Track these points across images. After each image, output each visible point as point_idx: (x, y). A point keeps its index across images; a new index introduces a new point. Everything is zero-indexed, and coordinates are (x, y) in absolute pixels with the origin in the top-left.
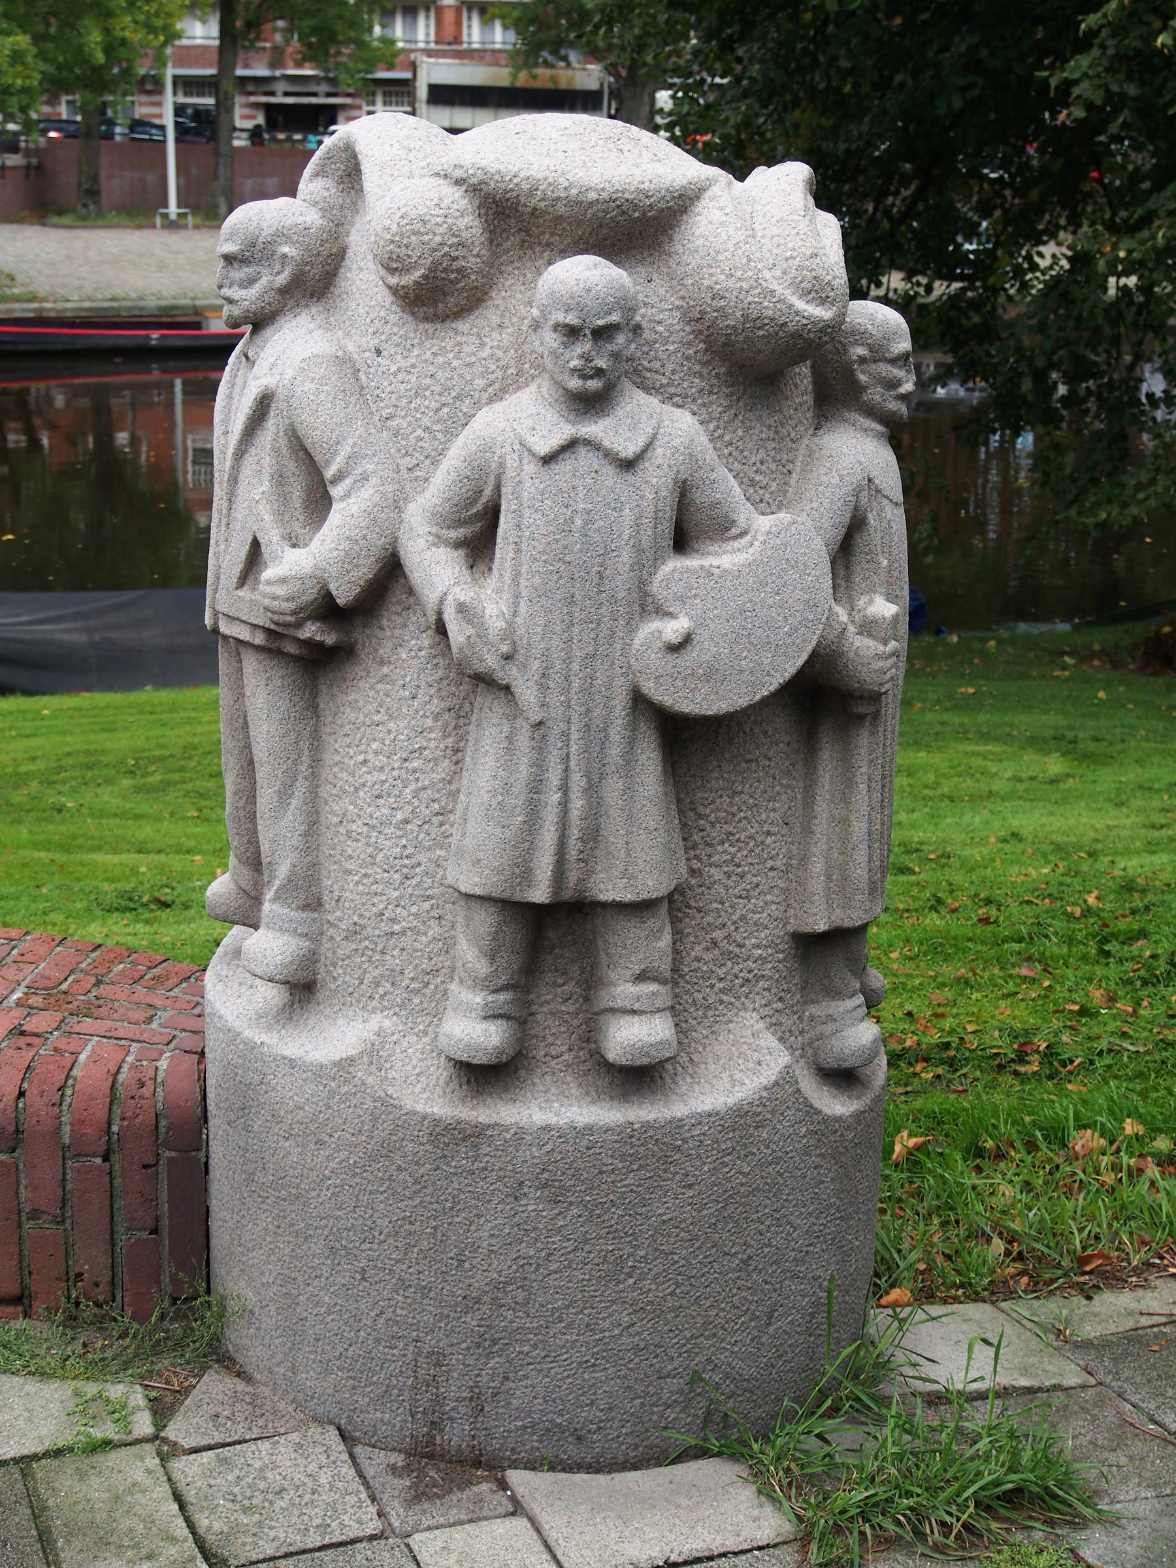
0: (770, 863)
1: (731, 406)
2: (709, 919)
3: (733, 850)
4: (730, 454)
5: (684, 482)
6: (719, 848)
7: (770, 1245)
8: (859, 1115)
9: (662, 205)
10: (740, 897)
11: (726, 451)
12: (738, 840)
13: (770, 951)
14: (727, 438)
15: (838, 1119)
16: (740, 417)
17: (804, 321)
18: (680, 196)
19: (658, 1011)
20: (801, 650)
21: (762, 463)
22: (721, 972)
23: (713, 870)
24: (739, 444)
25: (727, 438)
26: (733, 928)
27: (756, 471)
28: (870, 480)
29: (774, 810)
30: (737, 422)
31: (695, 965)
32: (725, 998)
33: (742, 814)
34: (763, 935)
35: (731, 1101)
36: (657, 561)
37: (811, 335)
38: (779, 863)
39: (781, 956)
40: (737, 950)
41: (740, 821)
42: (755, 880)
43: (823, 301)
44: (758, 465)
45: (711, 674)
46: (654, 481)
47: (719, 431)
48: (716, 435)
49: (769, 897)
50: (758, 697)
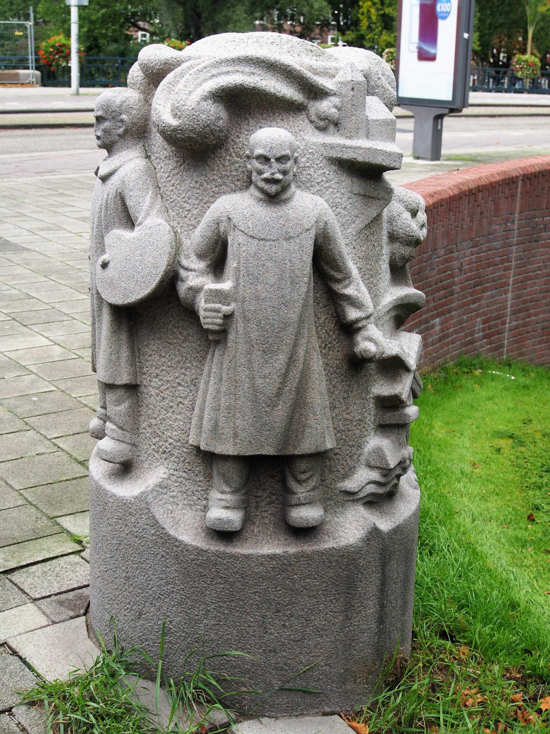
0: (179, 400)
1: (176, 167)
2: (150, 412)
3: (160, 383)
4: (172, 190)
5: (120, 193)
6: (154, 379)
7: (138, 578)
8: (200, 551)
9: (157, 67)
10: (162, 408)
11: (171, 188)
12: (162, 379)
13: (178, 444)
14: (172, 182)
15: (180, 542)
16: (181, 173)
17: (164, 125)
18: (165, 63)
19: (113, 439)
20: (147, 286)
21: (189, 199)
22: (154, 440)
23: (151, 389)
24: (178, 186)
25: (172, 182)
26: (159, 422)
27: (185, 202)
28: (229, 219)
29: (185, 375)
30: (179, 175)
31: (144, 431)
32: (155, 454)
33: (164, 368)
34: (174, 433)
35: (122, 494)
36: (108, 228)
37: (169, 133)
38: (186, 403)
39: (185, 450)
40: (161, 434)
41: (162, 370)
42: (171, 404)
43: (175, 116)
44: (186, 199)
45: (111, 284)
46: (109, 189)
47: (170, 178)
48: (168, 179)
49: (179, 416)
50: (126, 302)
